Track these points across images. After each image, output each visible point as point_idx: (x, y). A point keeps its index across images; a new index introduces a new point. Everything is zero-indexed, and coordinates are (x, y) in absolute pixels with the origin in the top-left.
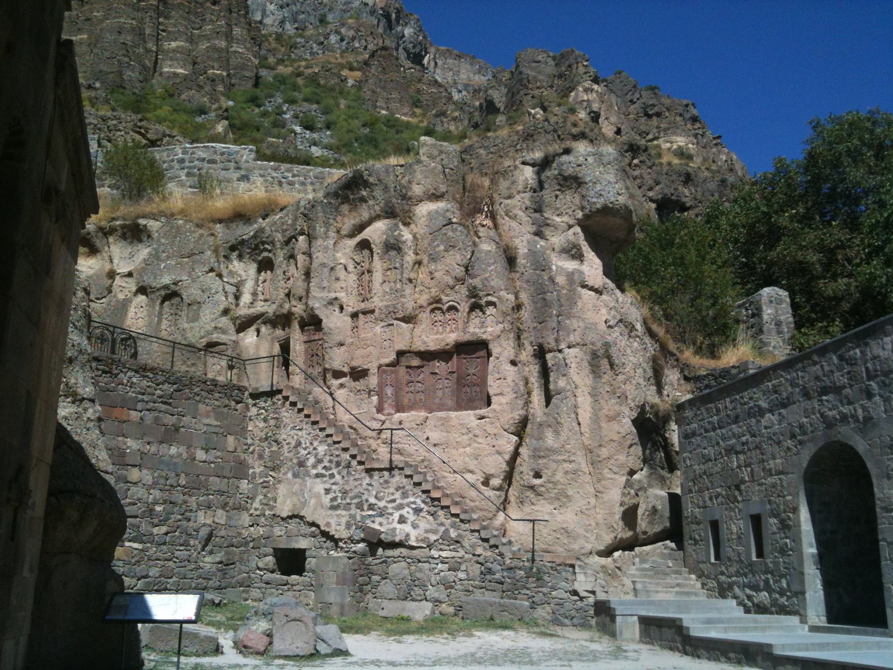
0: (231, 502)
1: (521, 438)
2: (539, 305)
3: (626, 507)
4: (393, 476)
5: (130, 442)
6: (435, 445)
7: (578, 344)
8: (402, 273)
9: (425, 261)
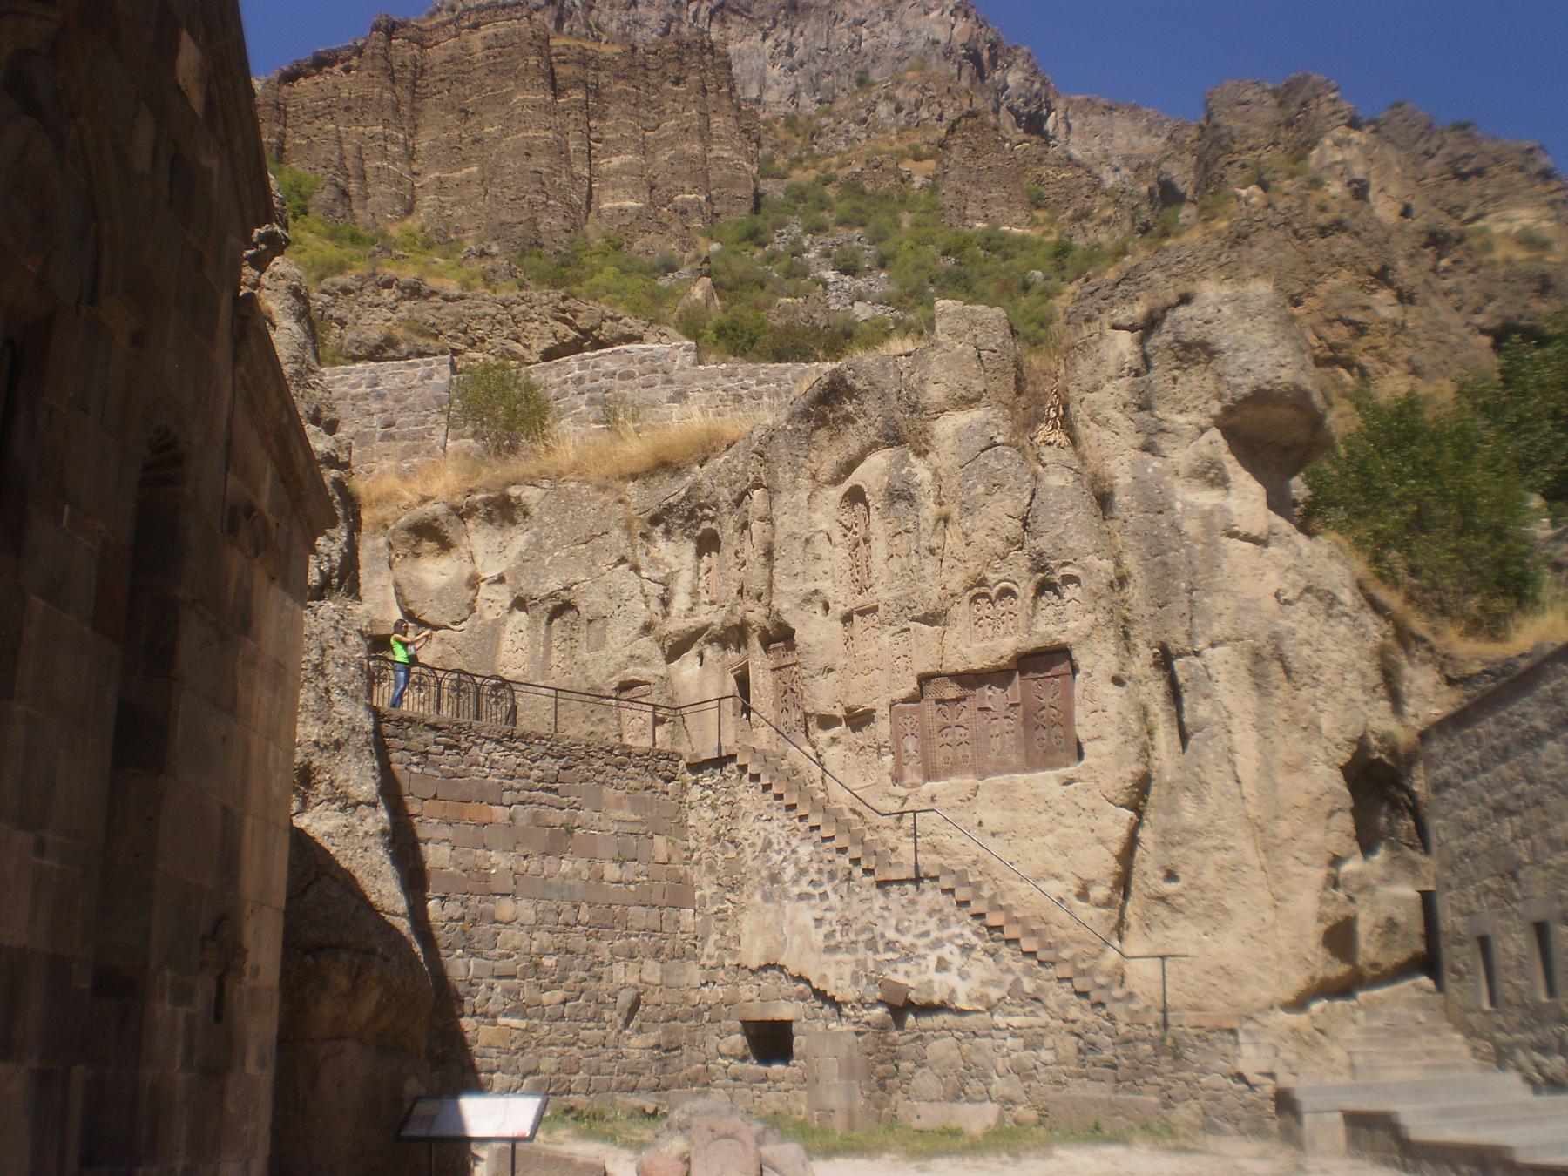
0: (668, 947)
1: (1140, 813)
2: (1156, 575)
3: (1330, 923)
4: (923, 891)
5: (495, 857)
6: (993, 834)
7: (1228, 639)
8: (918, 540)
9: (955, 515)
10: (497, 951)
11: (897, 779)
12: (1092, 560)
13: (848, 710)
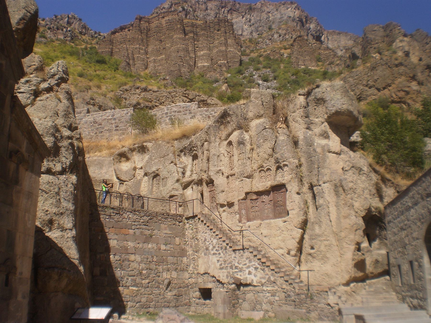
0: (179, 268)
2: (309, 164)
3: (356, 261)
4: (245, 252)
5: (130, 243)
6: (265, 237)
7: (328, 181)
9: (255, 148)
10: (130, 269)
11: (240, 221)
12: (291, 160)
13: (228, 202)
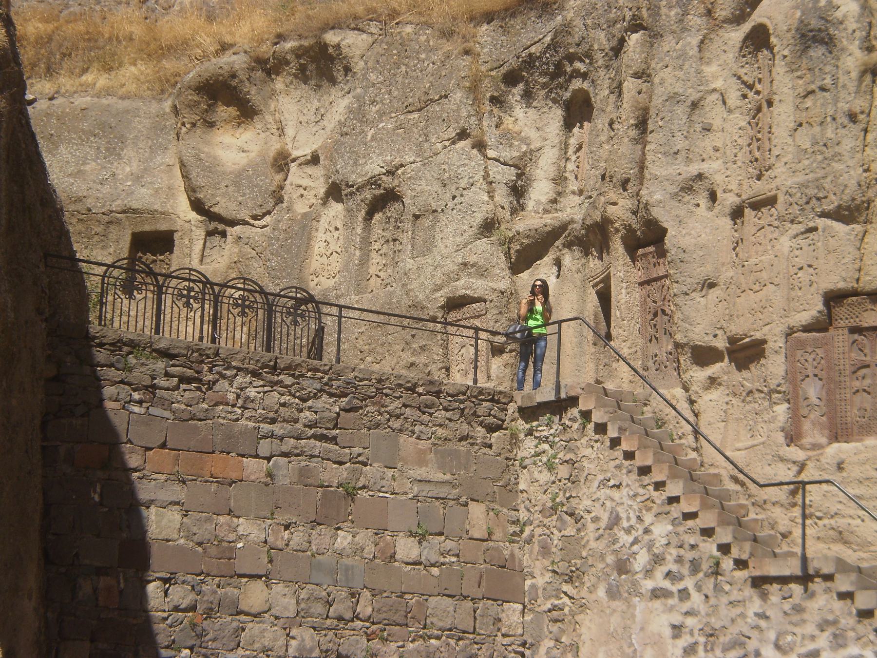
4: (812, 595)
5: (244, 526)
8: (836, 100)
11: (793, 437)
13: (732, 340)
